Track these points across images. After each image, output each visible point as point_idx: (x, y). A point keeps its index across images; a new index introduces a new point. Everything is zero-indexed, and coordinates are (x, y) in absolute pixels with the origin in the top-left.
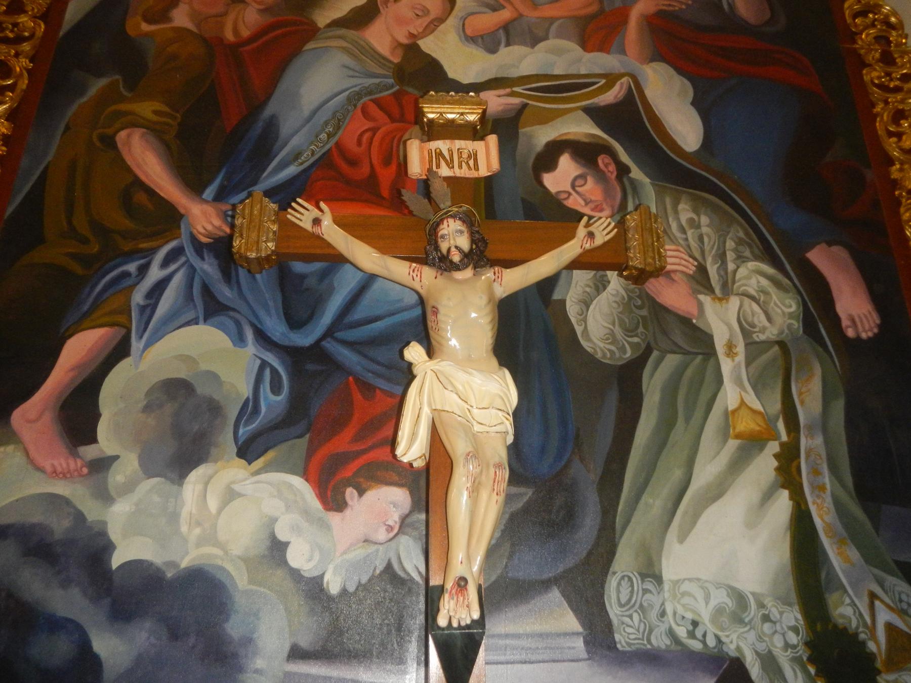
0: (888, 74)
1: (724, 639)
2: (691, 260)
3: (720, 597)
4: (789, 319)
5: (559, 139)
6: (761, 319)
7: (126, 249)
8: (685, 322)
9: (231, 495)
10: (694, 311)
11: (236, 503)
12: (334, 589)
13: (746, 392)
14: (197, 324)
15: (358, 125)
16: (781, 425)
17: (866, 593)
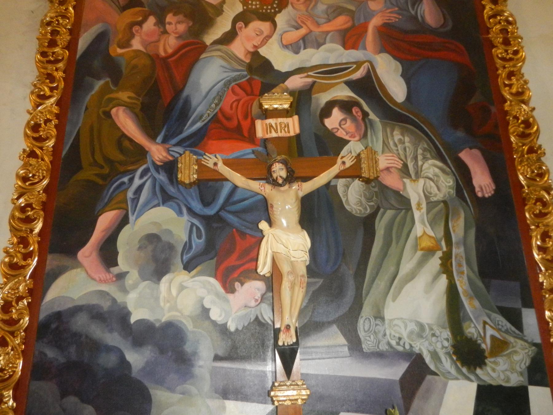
0: (506, 51)
1: (413, 345)
2: (400, 161)
3: (412, 326)
4: (449, 189)
5: (332, 100)
7: (122, 170)
8: (397, 193)
9: (182, 288)
10: (401, 188)
11: (185, 291)
12: (232, 328)
13: (426, 226)
14: (159, 206)
15: (230, 98)
16: (443, 243)
17: (482, 322)
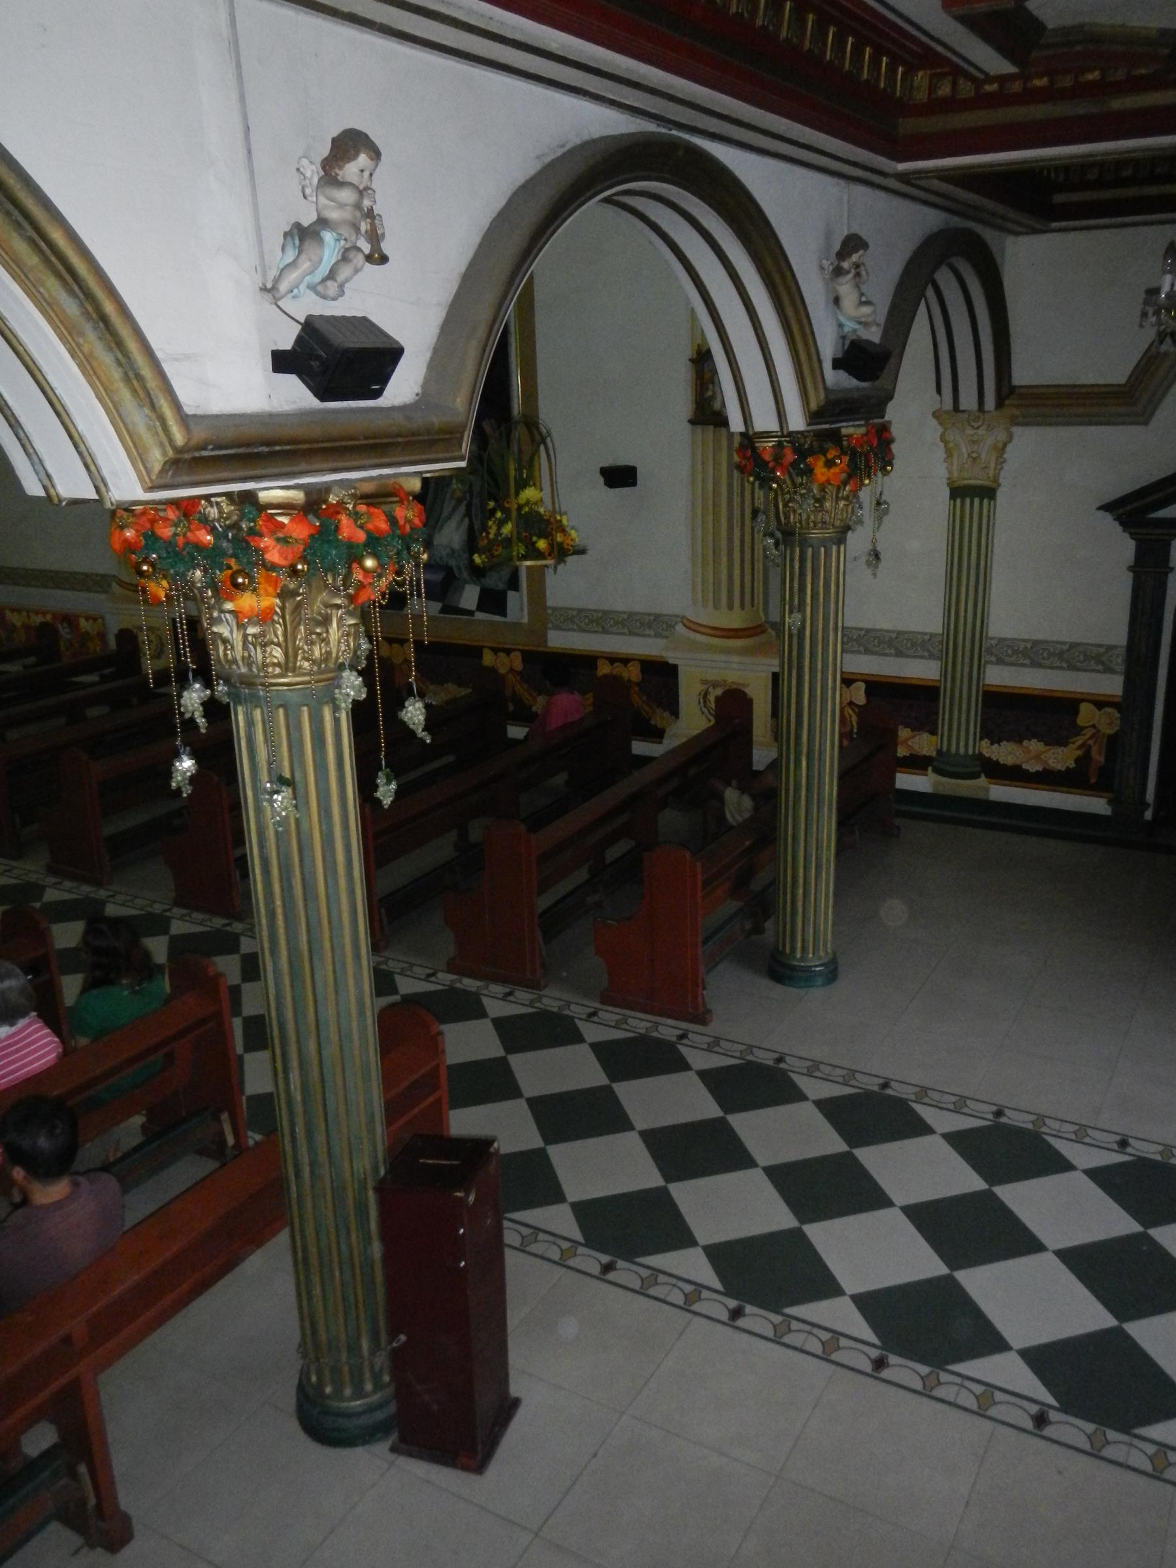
3: (448, 550)
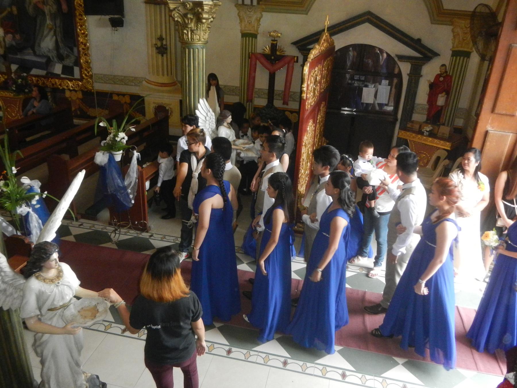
3: (47, 49)
6: (52, 10)
